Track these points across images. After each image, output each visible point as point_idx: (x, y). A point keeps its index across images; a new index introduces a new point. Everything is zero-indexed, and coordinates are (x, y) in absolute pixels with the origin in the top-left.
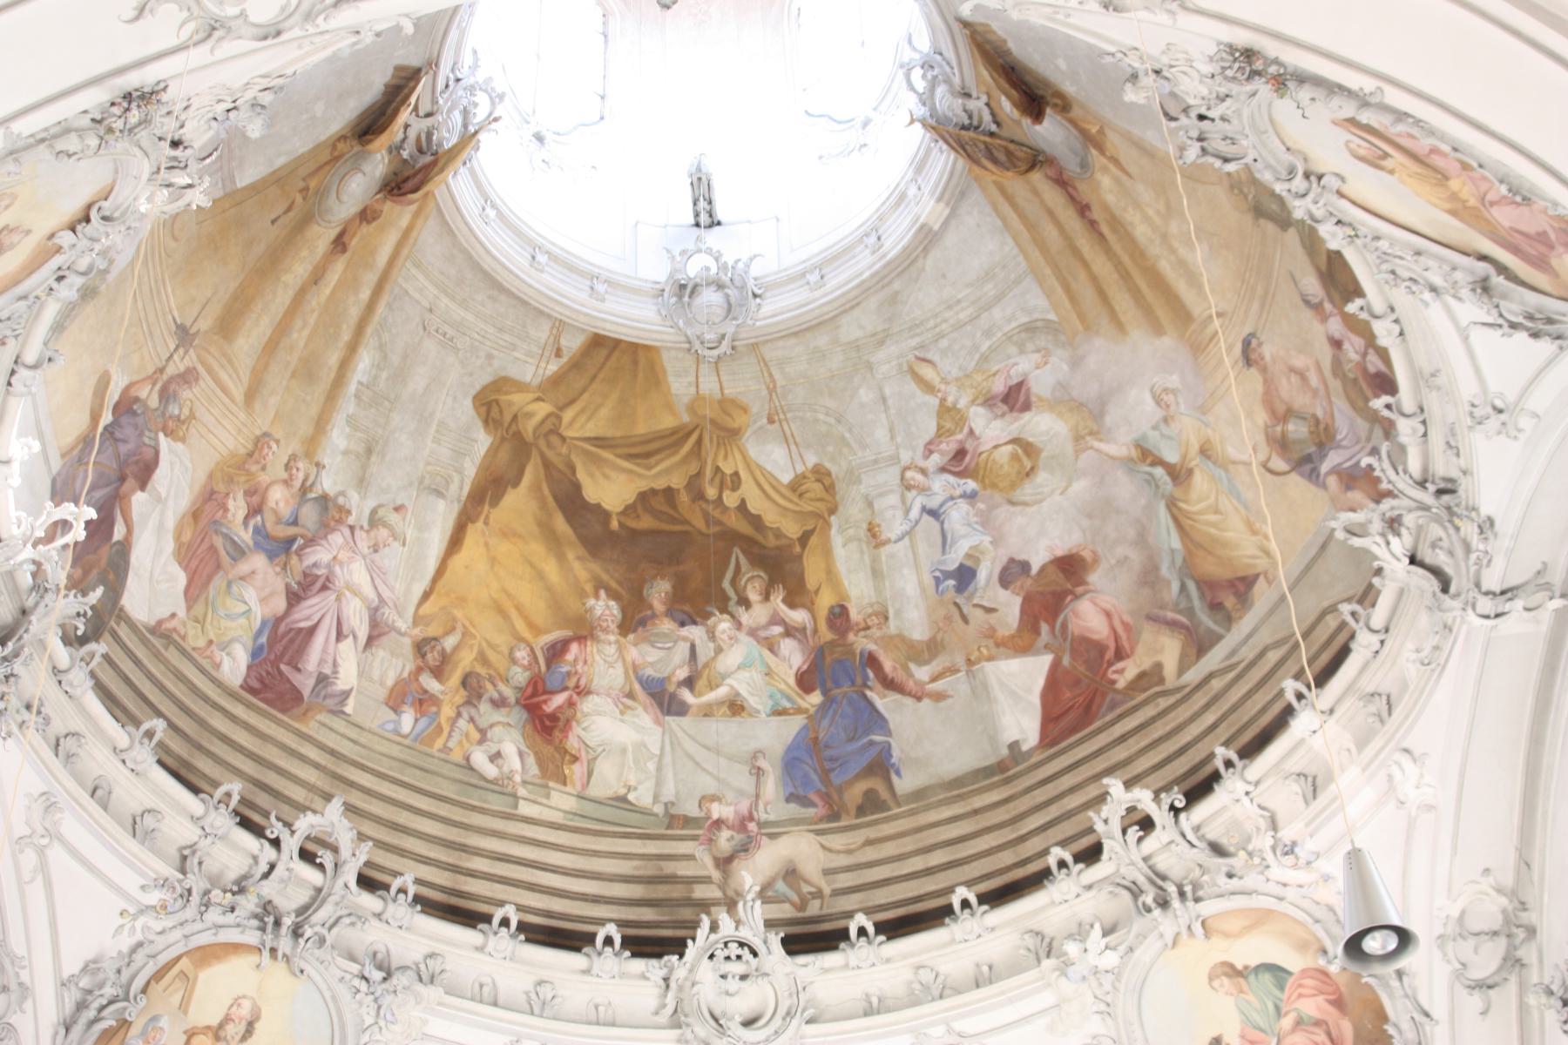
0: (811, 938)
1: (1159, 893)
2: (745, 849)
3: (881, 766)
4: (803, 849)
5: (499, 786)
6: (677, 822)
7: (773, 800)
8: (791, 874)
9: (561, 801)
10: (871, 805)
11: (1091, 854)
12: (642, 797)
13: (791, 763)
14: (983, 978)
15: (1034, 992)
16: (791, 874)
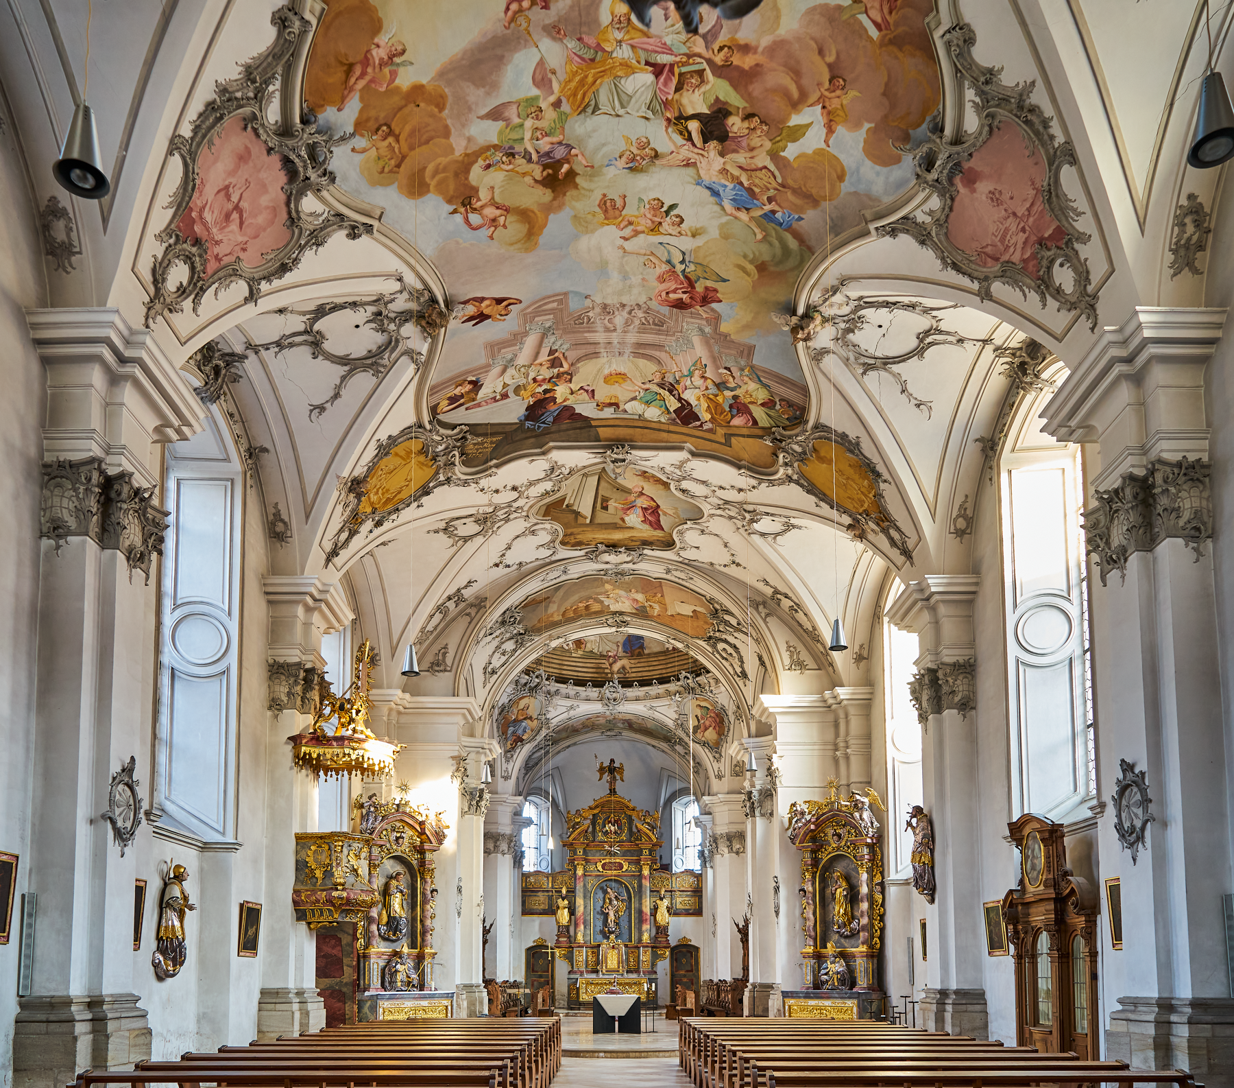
0: (626, 684)
1: (689, 690)
2: (615, 662)
3: (642, 647)
4: (625, 662)
5: (568, 651)
6: (602, 656)
7: (621, 653)
8: (623, 668)
9: (580, 652)
10: (640, 655)
11: (678, 680)
12: (595, 651)
13: (624, 645)
14: (658, 697)
15: (665, 701)
16: (623, 668)
